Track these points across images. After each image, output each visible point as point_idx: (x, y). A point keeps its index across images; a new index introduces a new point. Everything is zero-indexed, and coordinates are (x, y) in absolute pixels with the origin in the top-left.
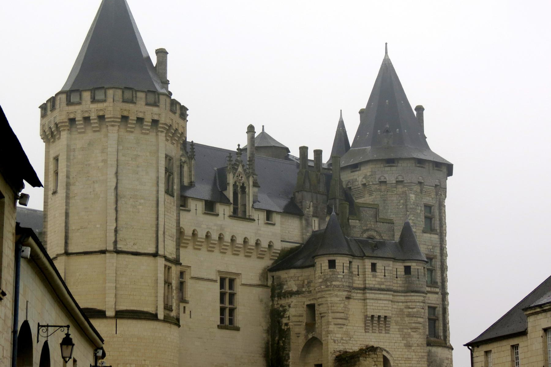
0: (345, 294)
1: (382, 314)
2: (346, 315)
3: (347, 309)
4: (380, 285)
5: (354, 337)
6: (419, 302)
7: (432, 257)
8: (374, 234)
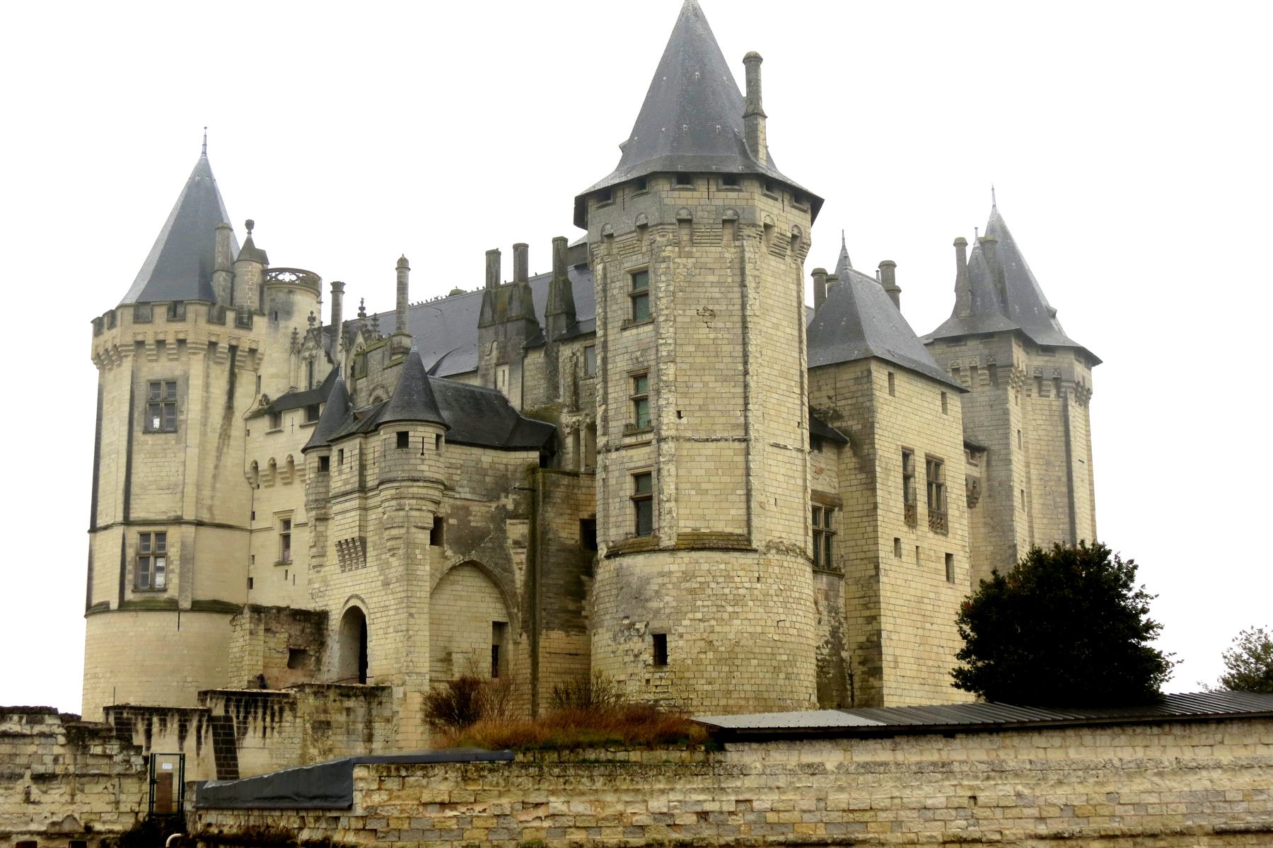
0: (313, 513)
1: (348, 537)
2: (320, 550)
3: (321, 539)
4: (345, 485)
5: (331, 583)
6: (386, 500)
7: (642, 372)
8: (380, 392)
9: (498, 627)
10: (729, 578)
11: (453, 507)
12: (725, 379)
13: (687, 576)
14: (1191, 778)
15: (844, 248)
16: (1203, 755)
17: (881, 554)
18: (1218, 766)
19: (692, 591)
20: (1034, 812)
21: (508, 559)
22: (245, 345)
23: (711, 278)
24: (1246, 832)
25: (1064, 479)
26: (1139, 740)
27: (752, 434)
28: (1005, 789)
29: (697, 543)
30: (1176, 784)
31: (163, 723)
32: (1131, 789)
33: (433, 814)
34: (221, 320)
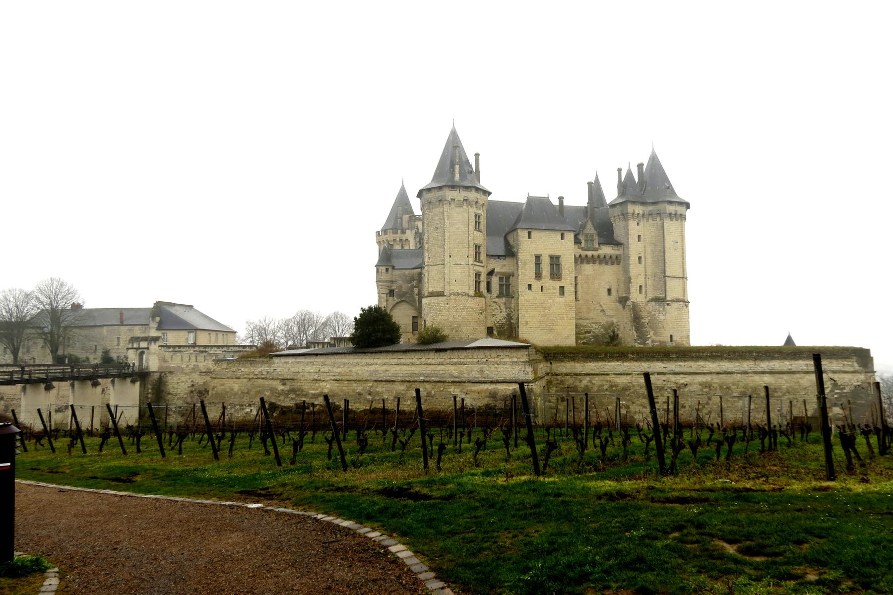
9: (413, 317)
10: (438, 304)
11: (397, 287)
12: (439, 247)
13: (429, 304)
14: (370, 367)
15: (597, 175)
16: (375, 361)
17: (519, 290)
18: (376, 364)
19: (430, 308)
20: (333, 374)
21: (414, 299)
22: (404, 239)
23: (437, 218)
24: (381, 381)
25: (662, 250)
26: (360, 357)
27: (445, 262)
28: (326, 368)
29: (431, 295)
30: (366, 368)
31: (318, 346)
32: (355, 369)
33: (224, 371)
34: (397, 233)
